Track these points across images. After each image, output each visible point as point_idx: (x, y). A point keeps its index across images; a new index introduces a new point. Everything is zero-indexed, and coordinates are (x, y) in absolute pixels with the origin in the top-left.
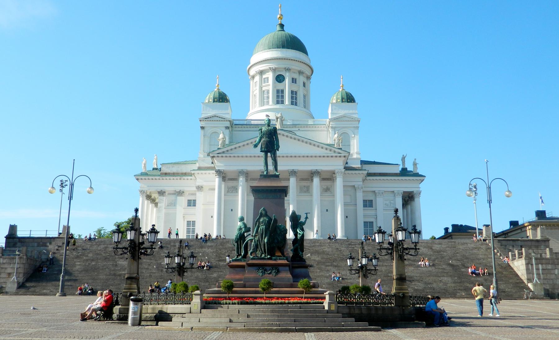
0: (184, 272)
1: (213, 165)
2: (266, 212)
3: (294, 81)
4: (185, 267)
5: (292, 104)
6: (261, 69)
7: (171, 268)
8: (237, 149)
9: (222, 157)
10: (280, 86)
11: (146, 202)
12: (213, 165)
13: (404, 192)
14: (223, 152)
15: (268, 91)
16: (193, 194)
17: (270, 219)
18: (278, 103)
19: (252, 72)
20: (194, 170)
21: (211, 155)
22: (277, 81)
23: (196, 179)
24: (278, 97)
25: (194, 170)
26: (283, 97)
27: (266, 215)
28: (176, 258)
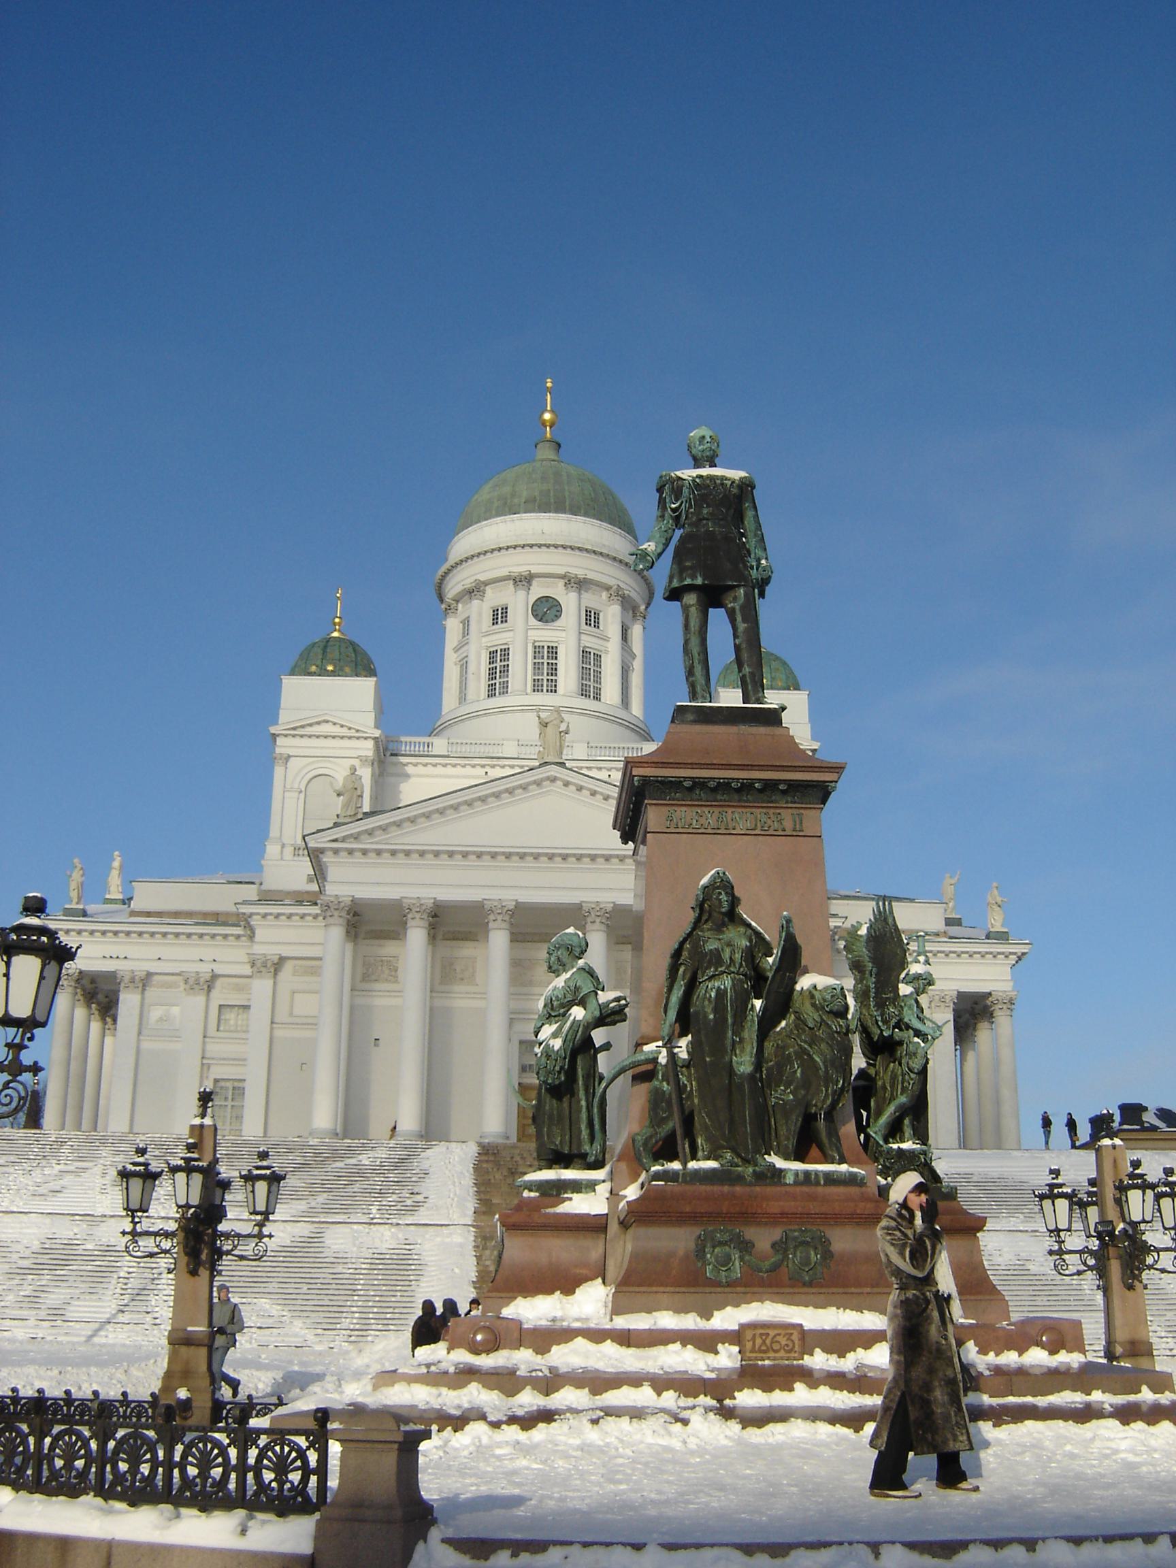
0: (219, 1253)
1: (314, 887)
2: (734, 901)
3: (592, 618)
4: (223, 1227)
5: (584, 693)
6: (482, 577)
7: (156, 1234)
8: (408, 828)
9: (351, 852)
10: (544, 634)
11: (80, 1012)
12: (314, 887)
13: (961, 996)
14: (356, 837)
15: (505, 652)
16: (239, 989)
17: (759, 944)
18: (537, 688)
19: (453, 587)
20: (245, 903)
21: (312, 844)
22: (535, 616)
23: (252, 937)
24: (537, 667)
25: (245, 903)
26: (553, 670)
27: (732, 916)
28: (181, 1177)
